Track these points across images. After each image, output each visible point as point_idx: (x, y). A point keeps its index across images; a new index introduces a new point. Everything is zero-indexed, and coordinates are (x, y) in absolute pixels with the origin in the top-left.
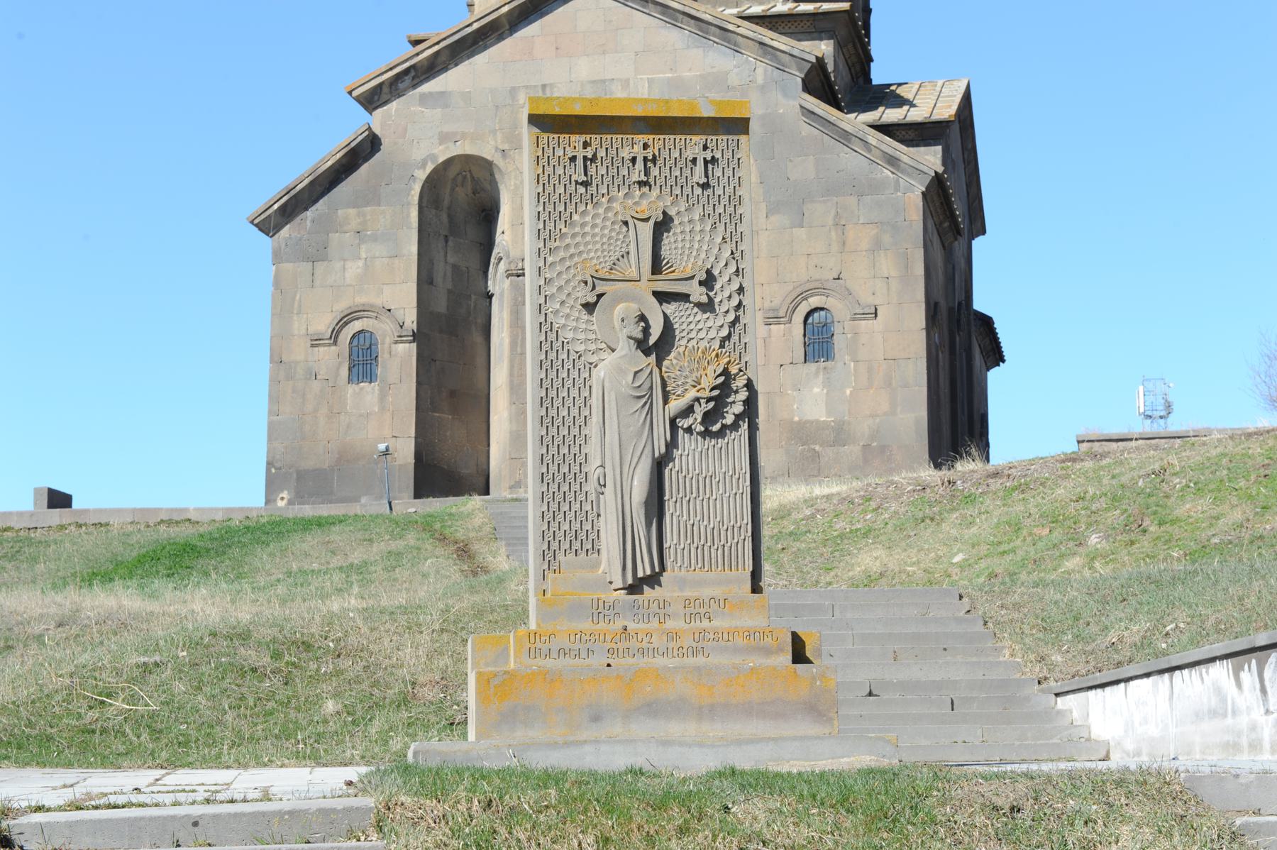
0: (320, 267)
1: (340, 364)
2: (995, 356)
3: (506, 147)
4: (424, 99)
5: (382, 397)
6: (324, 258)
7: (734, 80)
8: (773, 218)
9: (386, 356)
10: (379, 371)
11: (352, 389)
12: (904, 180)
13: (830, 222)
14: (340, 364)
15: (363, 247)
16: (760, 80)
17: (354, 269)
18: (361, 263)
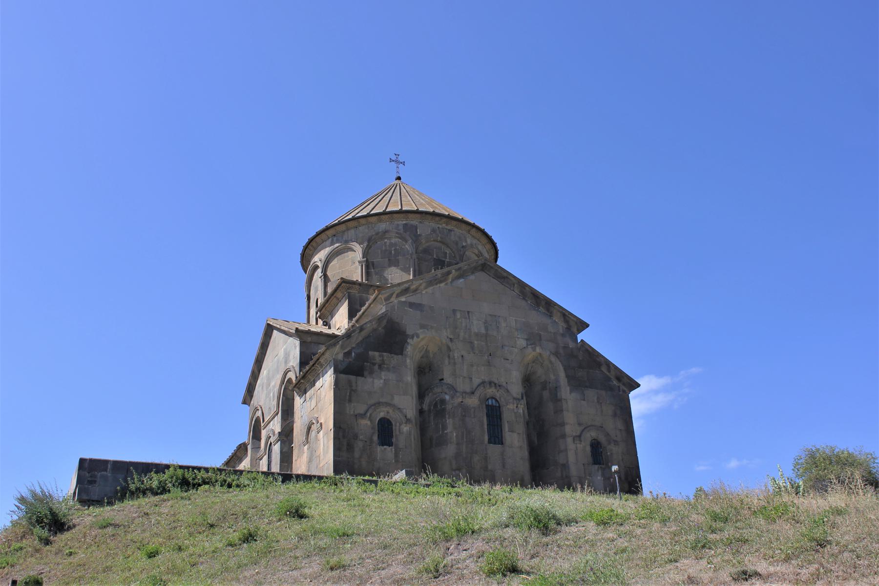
1: (373, 433)
3: (452, 337)
4: (412, 305)
5: (396, 455)
6: (362, 376)
7: (551, 329)
8: (573, 394)
9: (398, 433)
10: (394, 440)
11: (379, 449)
12: (622, 387)
13: (595, 398)
14: (373, 433)
15: (383, 373)
16: (561, 331)
17: (378, 383)
18: (382, 381)
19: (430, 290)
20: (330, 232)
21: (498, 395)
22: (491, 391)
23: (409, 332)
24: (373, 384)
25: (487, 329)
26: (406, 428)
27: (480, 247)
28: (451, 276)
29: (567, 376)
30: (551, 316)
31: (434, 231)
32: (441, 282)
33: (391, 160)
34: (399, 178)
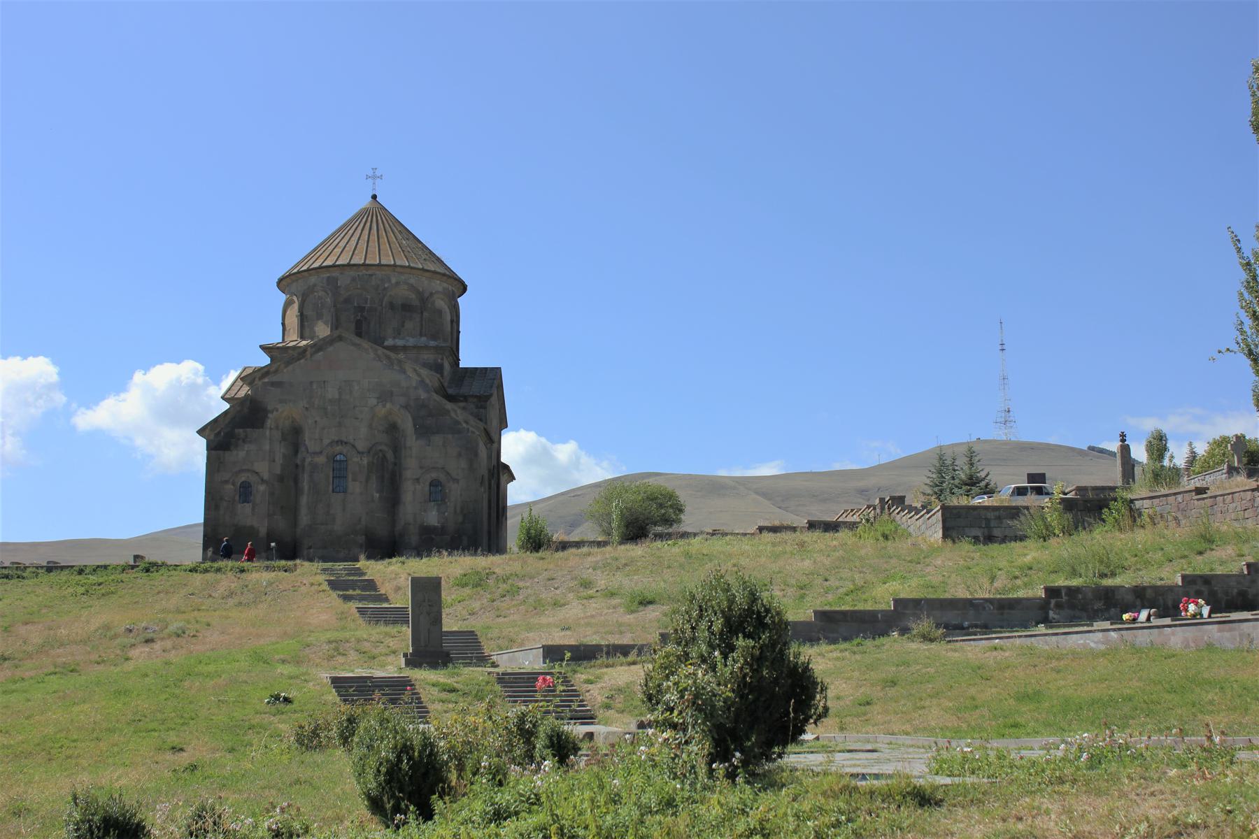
0: (227, 453)
2: (512, 478)
4: (273, 384)
5: (253, 509)
11: (240, 506)
17: (242, 454)
19: (291, 367)
20: (284, 282)
21: (345, 451)
22: (338, 448)
23: (269, 408)
24: (238, 454)
25: (340, 394)
26: (262, 488)
27: (412, 281)
28: (308, 353)
29: (415, 425)
30: (405, 372)
31: (354, 279)
32: (299, 359)
33: (368, 177)
34: (374, 197)
